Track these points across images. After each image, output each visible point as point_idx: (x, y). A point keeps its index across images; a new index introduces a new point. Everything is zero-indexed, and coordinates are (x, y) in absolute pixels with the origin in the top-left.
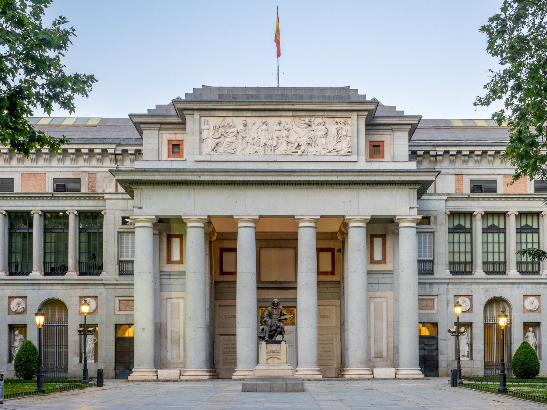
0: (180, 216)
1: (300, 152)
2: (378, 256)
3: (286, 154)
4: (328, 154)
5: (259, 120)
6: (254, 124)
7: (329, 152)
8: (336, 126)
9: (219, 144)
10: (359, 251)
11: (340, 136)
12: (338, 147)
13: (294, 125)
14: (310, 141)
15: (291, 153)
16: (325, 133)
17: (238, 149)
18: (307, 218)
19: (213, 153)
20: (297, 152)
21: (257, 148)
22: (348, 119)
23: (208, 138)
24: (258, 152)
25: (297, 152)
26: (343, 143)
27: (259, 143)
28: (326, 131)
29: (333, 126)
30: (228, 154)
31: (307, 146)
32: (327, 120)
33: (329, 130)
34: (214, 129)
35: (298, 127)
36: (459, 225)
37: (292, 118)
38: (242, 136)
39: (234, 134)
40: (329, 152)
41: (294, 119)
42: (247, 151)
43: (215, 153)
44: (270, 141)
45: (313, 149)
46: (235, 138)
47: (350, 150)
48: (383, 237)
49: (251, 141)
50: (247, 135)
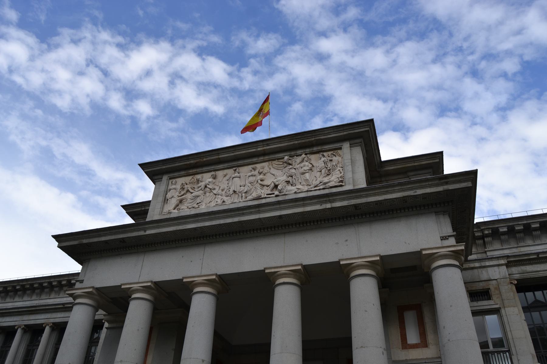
0: (120, 286)
1: (277, 193)
2: (413, 337)
3: (259, 198)
4: (313, 189)
5: (230, 172)
6: (225, 176)
7: (315, 187)
8: (323, 159)
9: (183, 201)
10: (366, 311)
11: (328, 169)
12: (326, 180)
13: (272, 168)
14: (290, 179)
15: (266, 196)
16: (308, 168)
17: (204, 204)
18: (283, 270)
19: (176, 211)
20: (274, 194)
21: (225, 199)
22: (339, 151)
23: (173, 197)
24: (226, 201)
25: (274, 194)
26: (333, 174)
27: (228, 193)
28: (310, 166)
29: (319, 161)
30: (191, 209)
31: (286, 184)
32: (313, 157)
33: (314, 165)
34: (181, 189)
35: (277, 169)
36: (536, 301)
37: (270, 162)
38: (209, 188)
39: (200, 188)
40: (315, 187)
41: (272, 163)
42: (213, 204)
43: (177, 211)
44: (242, 187)
45: (293, 188)
46: (201, 192)
47: (341, 179)
48: (418, 309)
49: (220, 192)
50: (216, 187)
